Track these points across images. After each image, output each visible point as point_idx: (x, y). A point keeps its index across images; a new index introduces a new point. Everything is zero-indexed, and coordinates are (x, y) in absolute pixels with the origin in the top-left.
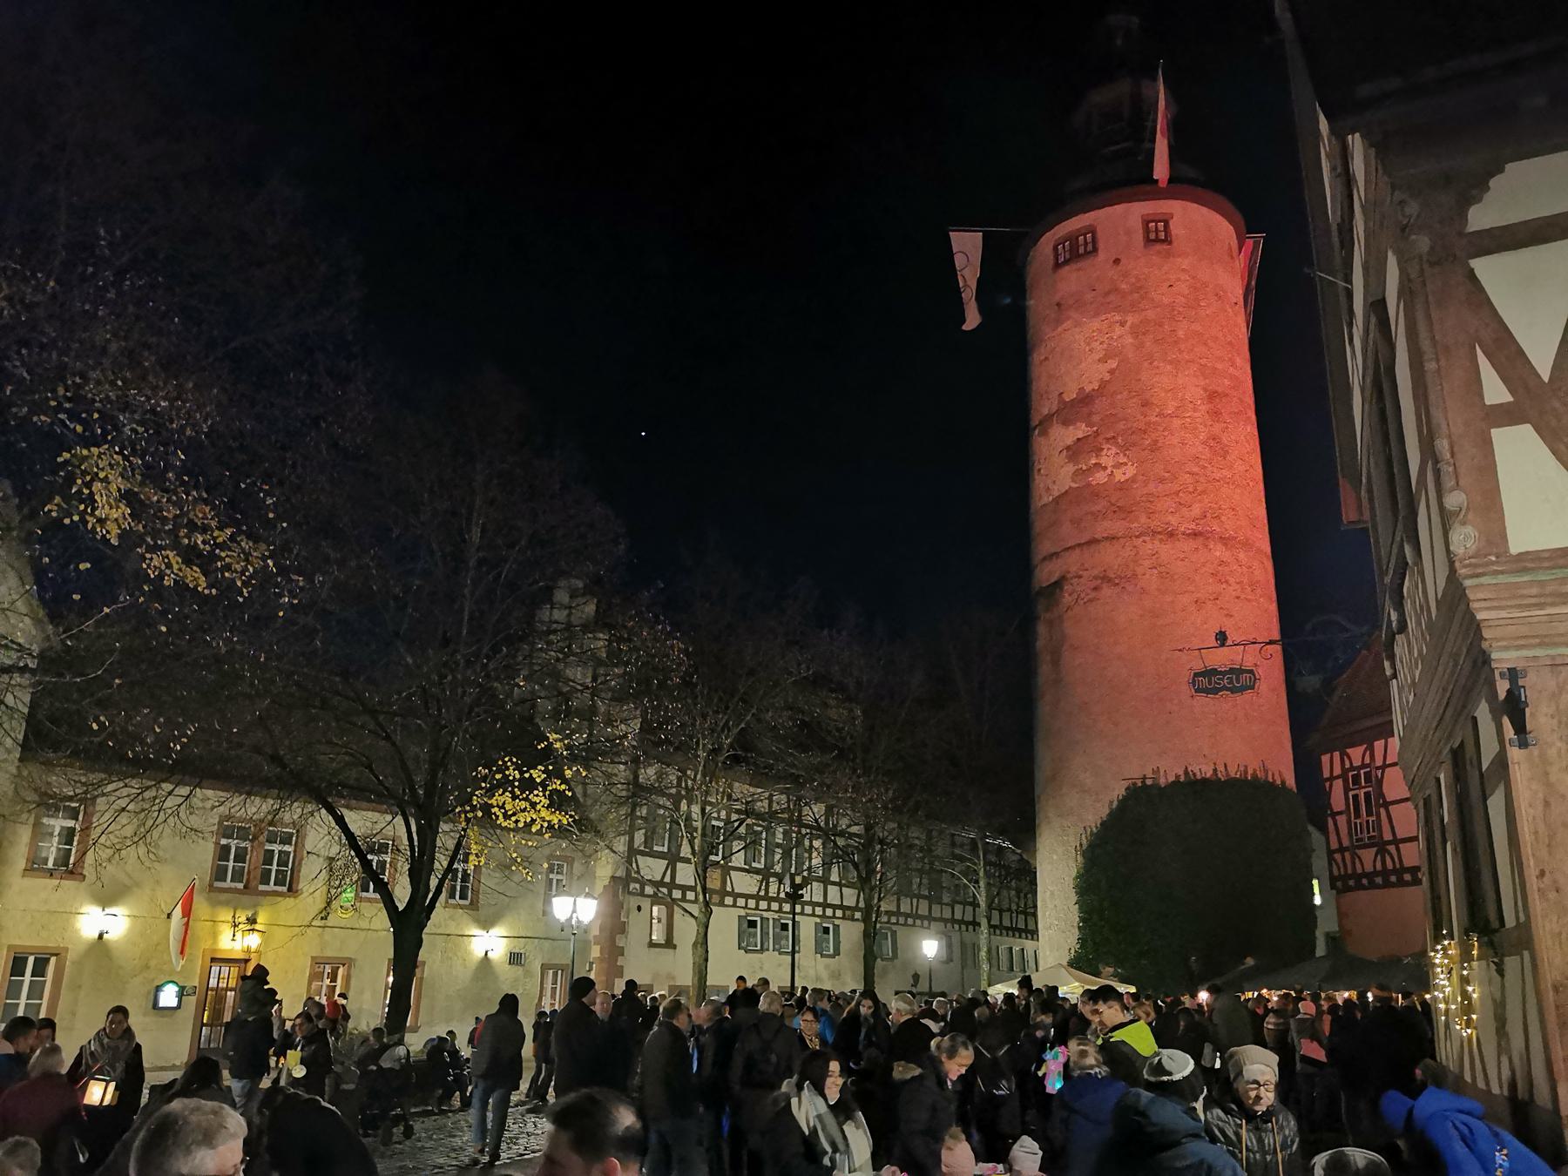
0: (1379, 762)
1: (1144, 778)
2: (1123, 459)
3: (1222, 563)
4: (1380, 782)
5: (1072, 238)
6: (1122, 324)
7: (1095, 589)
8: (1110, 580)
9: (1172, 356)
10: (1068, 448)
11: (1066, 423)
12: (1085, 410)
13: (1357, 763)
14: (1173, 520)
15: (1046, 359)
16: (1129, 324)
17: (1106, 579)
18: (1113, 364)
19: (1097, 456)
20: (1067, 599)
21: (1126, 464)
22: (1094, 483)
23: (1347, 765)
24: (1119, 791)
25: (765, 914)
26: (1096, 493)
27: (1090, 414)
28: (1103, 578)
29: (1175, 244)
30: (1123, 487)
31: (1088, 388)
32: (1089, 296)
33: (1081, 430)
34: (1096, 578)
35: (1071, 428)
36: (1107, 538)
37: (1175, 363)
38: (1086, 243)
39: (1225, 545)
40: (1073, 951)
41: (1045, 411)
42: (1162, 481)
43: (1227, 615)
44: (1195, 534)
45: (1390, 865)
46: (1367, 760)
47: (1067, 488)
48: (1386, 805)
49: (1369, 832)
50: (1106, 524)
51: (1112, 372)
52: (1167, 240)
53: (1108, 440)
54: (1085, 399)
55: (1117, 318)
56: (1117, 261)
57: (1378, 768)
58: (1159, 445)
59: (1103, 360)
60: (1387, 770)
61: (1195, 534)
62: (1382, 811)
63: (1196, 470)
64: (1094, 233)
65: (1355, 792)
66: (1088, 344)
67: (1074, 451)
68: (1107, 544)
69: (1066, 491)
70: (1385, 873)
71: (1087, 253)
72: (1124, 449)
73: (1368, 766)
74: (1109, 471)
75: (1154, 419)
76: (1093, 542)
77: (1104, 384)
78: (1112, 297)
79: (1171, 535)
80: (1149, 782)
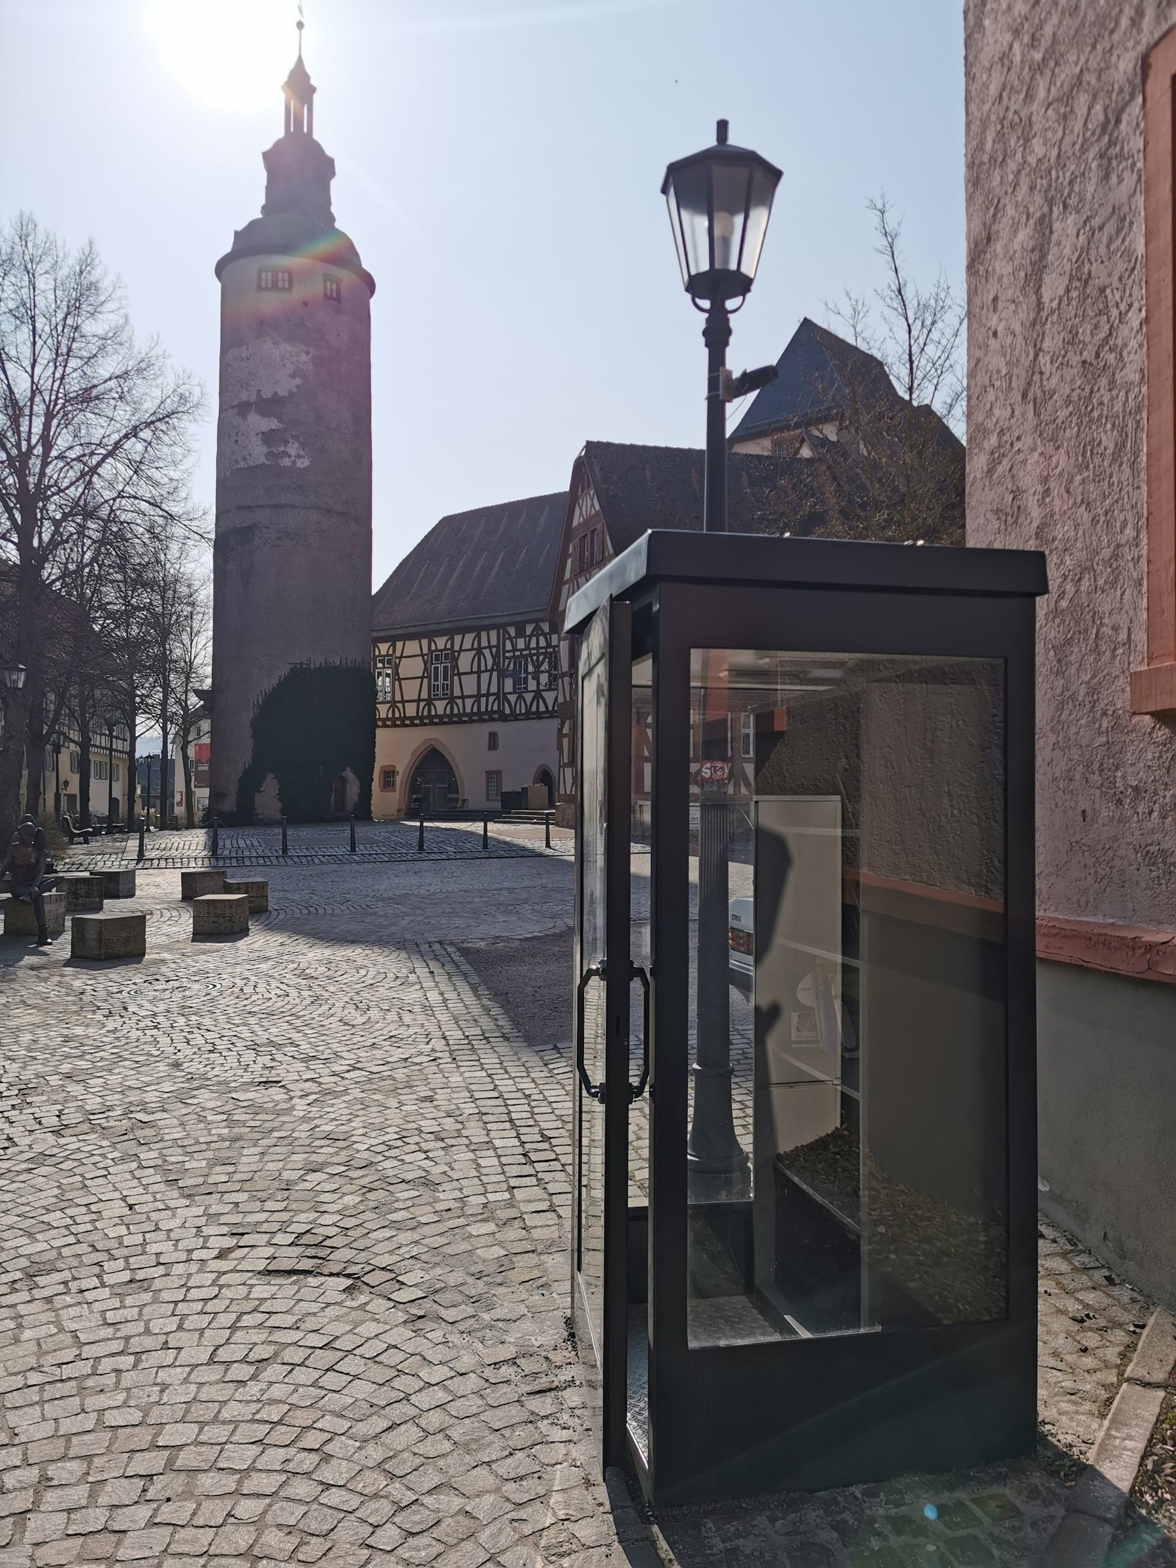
0: (398, 654)
1: (301, 664)
4: (397, 666)
6: (307, 353)
7: (278, 539)
10: (263, 433)
11: (263, 414)
13: (384, 652)
16: (311, 355)
18: (298, 381)
19: (285, 447)
24: (285, 670)
31: (281, 394)
33: (274, 424)
34: (279, 531)
40: (247, 765)
45: (397, 715)
48: (400, 680)
51: (298, 387)
53: (293, 437)
59: (293, 376)
61: (342, 514)
62: (397, 683)
67: (268, 438)
70: (394, 719)
71: (283, 289)
72: (304, 445)
73: (391, 655)
74: (292, 459)
76: (278, 506)
77: (291, 394)
79: (329, 511)
80: (304, 666)
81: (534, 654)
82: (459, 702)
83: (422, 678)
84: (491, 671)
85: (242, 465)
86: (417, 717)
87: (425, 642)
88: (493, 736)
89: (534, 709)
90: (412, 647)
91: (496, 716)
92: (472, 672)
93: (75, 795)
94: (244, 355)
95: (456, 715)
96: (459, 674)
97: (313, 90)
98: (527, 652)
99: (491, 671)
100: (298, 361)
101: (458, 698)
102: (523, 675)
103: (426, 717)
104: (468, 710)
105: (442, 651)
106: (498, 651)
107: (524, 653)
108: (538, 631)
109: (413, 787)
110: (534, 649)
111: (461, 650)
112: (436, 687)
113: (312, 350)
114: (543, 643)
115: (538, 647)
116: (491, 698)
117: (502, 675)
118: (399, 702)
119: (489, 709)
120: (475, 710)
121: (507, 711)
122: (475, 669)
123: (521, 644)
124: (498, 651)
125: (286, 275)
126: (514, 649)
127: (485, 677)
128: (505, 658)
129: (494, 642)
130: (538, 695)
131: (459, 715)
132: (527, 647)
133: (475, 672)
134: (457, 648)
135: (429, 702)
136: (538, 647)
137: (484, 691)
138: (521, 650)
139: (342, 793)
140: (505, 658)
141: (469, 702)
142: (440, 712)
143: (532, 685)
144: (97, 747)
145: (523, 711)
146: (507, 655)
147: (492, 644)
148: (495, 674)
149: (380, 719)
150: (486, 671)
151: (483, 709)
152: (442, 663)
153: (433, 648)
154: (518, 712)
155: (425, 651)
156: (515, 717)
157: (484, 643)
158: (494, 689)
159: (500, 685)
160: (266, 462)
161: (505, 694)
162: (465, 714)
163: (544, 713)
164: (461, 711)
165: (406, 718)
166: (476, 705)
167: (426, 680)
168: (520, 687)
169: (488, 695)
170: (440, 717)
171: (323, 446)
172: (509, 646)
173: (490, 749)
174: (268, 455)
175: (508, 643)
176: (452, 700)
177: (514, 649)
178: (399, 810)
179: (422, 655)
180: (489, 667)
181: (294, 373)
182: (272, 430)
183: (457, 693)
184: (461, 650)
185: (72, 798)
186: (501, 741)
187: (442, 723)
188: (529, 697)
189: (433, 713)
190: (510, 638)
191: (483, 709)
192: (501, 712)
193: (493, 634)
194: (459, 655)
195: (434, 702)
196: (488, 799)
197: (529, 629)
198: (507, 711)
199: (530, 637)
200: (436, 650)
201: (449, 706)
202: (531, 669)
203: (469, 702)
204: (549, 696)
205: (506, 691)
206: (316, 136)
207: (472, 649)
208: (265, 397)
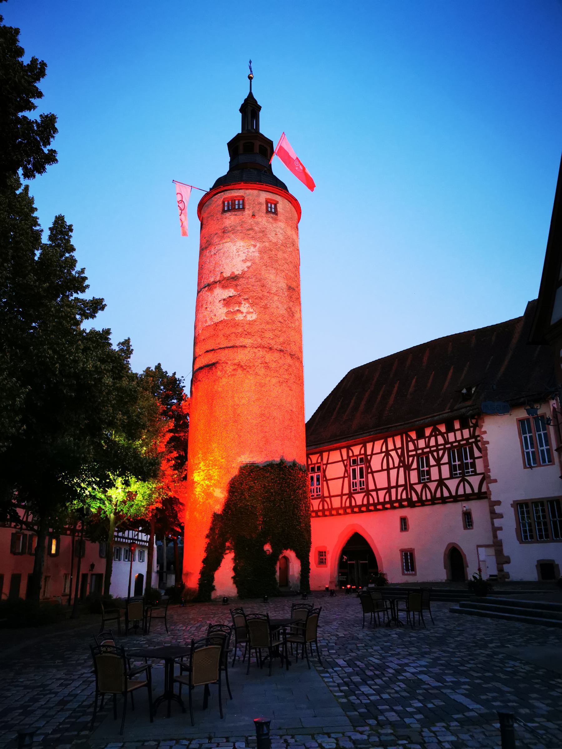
0: (325, 462)
2: (251, 310)
3: (290, 366)
4: (324, 471)
5: (233, 200)
6: (255, 246)
7: (234, 370)
8: (242, 367)
9: (275, 266)
10: (224, 300)
11: (224, 287)
12: (234, 283)
13: (314, 461)
14: (272, 342)
15: (215, 254)
16: (257, 248)
17: (239, 365)
18: (249, 264)
19: (239, 306)
20: (219, 373)
21: (252, 313)
22: (237, 319)
23: (310, 462)
25: (26, 532)
26: (236, 324)
27: (236, 286)
28: (238, 365)
29: (279, 215)
30: (251, 323)
32: (239, 228)
33: (231, 292)
34: (235, 364)
35: (227, 290)
36: (241, 346)
37: (276, 269)
38: (239, 204)
39: (292, 357)
41: (212, 280)
42: (268, 323)
43: (290, 390)
44: (281, 351)
45: (326, 507)
46: (319, 461)
47: (222, 319)
48: (327, 480)
49: (317, 492)
50: (242, 339)
51: (248, 268)
52: (276, 213)
53: (245, 299)
54: (234, 278)
55: (253, 243)
56: (254, 216)
57: (324, 464)
58: (268, 306)
59: (244, 261)
60: (328, 465)
61: (281, 351)
62: (325, 483)
63: (282, 321)
64: (243, 200)
65: (312, 475)
66: (238, 252)
67: (227, 302)
68: (241, 349)
69: (222, 321)
70: (323, 510)
72: (252, 305)
73: (320, 463)
75: (266, 294)
76: (233, 347)
77: (244, 273)
78: (251, 232)
79: (271, 349)
81: (434, 451)
82: (374, 494)
83: (344, 478)
84: (398, 467)
85: (209, 323)
86: (341, 507)
87: (344, 451)
88: (404, 521)
89: (438, 495)
90: (335, 456)
91: (405, 503)
92: (382, 470)
93: (102, 574)
94: (212, 253)
95: (372, 505)
96: (372, 472)
97: (259, 108)
98: (428, 450)
99: (398, 467)
100: (248, 252)
101: (373, 490)
102: (426, 469)
103: (348, 507)
104: (381, 500)
105: (357, 456)
106: (403, 452)
107: (425, 450)
108: (436, 433)
109: (342, 565)
110: (433, 447)
111: (372, 454)
112: (355, 484)
113: (258, 245)
114: (441, 440)
115: (437, 445)
116: (400, 489)
117: (408, 468)
118: (327, 497)
119: (399, 498)
120: (387, 499)
121: (415, 498)
122: (385, 467)
123: (422, 443)
124: (403, 452)
125: (241, 202)
126: (416, 449)
127: (393, 473)
128: (409, 456)
129: (399, 445)
130: (441, 482)
131: (375, 505)
132: (428, 446)
133: (385, 470)
134: (369, 452)
135: (350, 495)
136: (437, 445)
137: (393, 483)
138: (422, 449)
139: (285, 570)
140: (409, 456)
141: (382, 494)
142: (359, 502)
143: (434, 474)
144: (126, 538)
145: (429, 497)
146: (410, 453)
147: (397, 447)
148: (402, 470)
149: (313, 511)
150: (394, 468)
151: (394, 498)
152: (358, 465)
153: (351, 454)
154: (424, 498)
155: (345, 457)
156: (422, 503)
157: (391, 447)
158: (402, 481)
159: (407, 477)
160: (226, 318)
161: (411, 485)
162: (379, 503)
163: (447, 498)
164: (376, 501)
165: (332, 509)
166: (387, 495)
167: (346, 480)
168: (425, 477)
169: (397, 486)
170: (360, 507)
171: (266, 305)
172: (411, 446)
173: (402, 530)
174: (228, 313)
175: (411, 444)
176: (368, 493)
177: (416, 449)
178: (331, 582)
179: (343, 461)
180: (396, 465)
181: (246, 259)
182: (230, 297)
183: (371, 487)
184: (372, 454)
185: (99, 576)
186: (411, 523)
187: (361, 512)
188: (433, 486)
189: (353, 504)
190: (413, 441)
191: (394, 498)
192: (409, 500)
193: (398, 440)
194: (371, 458)
195: (354, 495)
196: (403, 574)
197: (428, 432)
198: (415, 498)
199: (429, 438)
200: (353, 456)
201: (366, 497)
202: (432, 462)
203: (382, 494)
204: (452, 484)
205: (412, 482)
206: (261, 131)
207: (382, 452)
208: (225, 276)
